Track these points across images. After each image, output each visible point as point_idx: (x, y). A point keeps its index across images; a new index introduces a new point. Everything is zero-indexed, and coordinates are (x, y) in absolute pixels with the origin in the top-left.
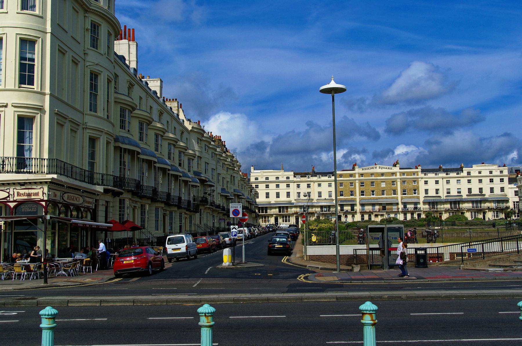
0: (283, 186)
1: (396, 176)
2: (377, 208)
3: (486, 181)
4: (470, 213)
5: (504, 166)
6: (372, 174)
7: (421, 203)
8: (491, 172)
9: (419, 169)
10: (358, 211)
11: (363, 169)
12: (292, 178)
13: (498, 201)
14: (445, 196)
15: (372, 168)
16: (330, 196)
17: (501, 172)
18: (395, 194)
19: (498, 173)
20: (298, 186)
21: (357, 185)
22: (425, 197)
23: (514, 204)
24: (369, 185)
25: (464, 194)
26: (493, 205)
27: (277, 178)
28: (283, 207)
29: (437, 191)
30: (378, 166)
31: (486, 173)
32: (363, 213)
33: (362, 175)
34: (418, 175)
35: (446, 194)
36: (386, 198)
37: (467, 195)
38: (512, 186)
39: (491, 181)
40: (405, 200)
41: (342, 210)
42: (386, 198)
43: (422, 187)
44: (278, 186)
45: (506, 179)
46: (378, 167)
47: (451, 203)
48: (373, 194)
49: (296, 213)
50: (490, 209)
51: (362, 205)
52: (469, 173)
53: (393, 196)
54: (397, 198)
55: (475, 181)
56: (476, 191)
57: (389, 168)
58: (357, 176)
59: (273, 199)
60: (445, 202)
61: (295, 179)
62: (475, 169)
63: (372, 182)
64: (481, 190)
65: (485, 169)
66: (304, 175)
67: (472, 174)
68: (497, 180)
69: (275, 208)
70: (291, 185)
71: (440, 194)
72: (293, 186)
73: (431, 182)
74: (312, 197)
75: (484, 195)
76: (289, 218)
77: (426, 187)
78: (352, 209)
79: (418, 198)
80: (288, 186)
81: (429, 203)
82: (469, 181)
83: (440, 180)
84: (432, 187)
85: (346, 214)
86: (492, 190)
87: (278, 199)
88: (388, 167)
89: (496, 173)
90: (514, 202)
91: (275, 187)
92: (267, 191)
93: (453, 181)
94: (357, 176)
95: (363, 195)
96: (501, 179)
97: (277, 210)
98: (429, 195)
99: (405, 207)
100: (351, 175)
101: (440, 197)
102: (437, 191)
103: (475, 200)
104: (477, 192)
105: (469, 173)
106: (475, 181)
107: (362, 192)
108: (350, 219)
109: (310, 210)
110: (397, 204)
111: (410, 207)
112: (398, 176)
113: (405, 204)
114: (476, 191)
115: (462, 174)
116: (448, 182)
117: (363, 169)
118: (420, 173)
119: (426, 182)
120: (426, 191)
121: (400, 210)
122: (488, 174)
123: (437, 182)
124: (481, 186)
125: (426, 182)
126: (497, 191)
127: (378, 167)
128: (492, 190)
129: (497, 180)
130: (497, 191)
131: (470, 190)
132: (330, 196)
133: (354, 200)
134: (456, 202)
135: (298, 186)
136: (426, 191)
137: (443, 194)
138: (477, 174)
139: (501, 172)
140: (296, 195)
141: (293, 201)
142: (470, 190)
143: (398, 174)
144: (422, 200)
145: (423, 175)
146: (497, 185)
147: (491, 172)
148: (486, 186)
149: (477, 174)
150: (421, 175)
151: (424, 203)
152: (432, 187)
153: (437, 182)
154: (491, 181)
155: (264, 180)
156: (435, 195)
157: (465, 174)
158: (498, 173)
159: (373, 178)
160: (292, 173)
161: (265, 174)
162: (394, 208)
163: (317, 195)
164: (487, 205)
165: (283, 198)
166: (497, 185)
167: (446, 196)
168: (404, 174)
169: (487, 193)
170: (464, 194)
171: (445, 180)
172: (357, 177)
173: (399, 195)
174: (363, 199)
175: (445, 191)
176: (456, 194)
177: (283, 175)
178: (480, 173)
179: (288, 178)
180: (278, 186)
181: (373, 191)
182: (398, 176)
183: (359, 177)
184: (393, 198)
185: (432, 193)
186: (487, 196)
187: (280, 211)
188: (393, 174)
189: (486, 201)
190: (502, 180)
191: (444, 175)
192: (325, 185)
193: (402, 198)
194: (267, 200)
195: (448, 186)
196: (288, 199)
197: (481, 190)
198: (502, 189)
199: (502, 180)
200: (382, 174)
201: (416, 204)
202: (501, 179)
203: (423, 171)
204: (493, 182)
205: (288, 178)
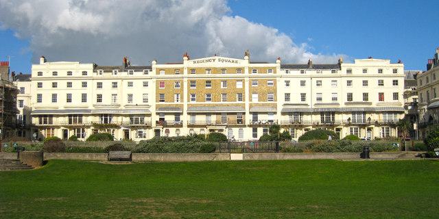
0: (77, 84)
1: (243, 73)
2: (213, 118)
3: (373, 83)
5: (399, 63)
8: (380, 71)
9: (278, 65)
12: (90, 73)
13: (390, 113)
14: (313, 104)
15: (209, 61)
16: (145, 100)
17: (395, 71)
18: (240, 99)
21: (185, 85)
22: (285, 105)
24: (204, 87)
25: (342, 103)
27: (70, 73)
29: (303, 96)
30: (217, 58)
31: (373, 71)
32: (191, 126)
33: (193, 71)
34: (275, 72)
35: (315, 101)
36: (231, 104)
37: (346, 104)
43: (281, 90)
45: (401, 82)
46: (217, 60)
47: (322, 113)
48: (209, 100)
49: (95, 125)
50: (377, 124)
52: (349, 71)
53: (238, 102)
55: (357, 83)
56: (358, 97)
57: (233, 62)
58: (186, 71)
62: (359, 65)
63: (208, 82)
64: (366, 96)
65: (373, 65)
67: (354, 73)
69: (64, 116)
70: (89, 83)
71: (308, 101)
72: (92, 85)
73: (295, 83)
74: (118, 102)
75: (370, 104)
77: (288, 90)
78: (177, 119)
79: (275, 106)
82: (349, 83)
83: (308, 81)
84: (295, 91)
86: (381, 97)
87: (69, 104)
88: (231, 59)
89: (388, 71)
92: (54, 92)
93: (326, 83)
94: (186, 71)
95: (193, 100)
97: (67, 119)
98: (292, 101)
99: (255, 119)
101: (307, 105)
102: (303, 96)
103: (357, 110)
104: (361, 99)
105: (349, 71)
106: (357, 83)
113: (255, 114)
114: (358, 97)
115: (339, 73)
117: (195, 62)
118: (278, 70)
119: (288, 84)
120: (287, 96)
121: (247, 123)
122: (376, 73)
123: (303, 83)
124: (365, 89)
125: (288, 84)
128: (381, 97)
131: (350, 97)
132: (145, 100)
133: (180, 107)
134: (328, 114)
136: (287, 96)
137: (311, 103)
139: (395, 71)
141: (91, 108)
142: (350, 97)
143: (247, 70)
144: (280, 109)
145: (283, 72)
147: (380, 71)
148: (373, 91)
151: (283, 114)
152: (295, 91)
153: (303, 83)
156: (300, 101)
157: (343, 71)
159: (210, 75)
160: (91, 66)
163: (126, 98)
164: (375, 117)
165: (77, 103)
167: (316, 104)
168: (255, 71)
169: (374, 100)
170: (342, 103)
171: (314, 80)
174: (193, 106)
175: (315, 96)
176: (331, 102)
177: (77, 68)
178: (365, 71)
179: (85, 73)
181: (209, 95)
183: (188, 73)
184: (237, 105)
185: (295, 99)
186: (374, 106)
188: (240, 70)
190: (395, 83)
191: (313, 73)
192: (138, 84)
193: (251, 106)
194: (54, 105)
195: (319, 89)
196: (84, 104)
197: (366, 96)
199: (395, 83)
200: (223, 70)
203: (283, 67)
204: (397, 84)
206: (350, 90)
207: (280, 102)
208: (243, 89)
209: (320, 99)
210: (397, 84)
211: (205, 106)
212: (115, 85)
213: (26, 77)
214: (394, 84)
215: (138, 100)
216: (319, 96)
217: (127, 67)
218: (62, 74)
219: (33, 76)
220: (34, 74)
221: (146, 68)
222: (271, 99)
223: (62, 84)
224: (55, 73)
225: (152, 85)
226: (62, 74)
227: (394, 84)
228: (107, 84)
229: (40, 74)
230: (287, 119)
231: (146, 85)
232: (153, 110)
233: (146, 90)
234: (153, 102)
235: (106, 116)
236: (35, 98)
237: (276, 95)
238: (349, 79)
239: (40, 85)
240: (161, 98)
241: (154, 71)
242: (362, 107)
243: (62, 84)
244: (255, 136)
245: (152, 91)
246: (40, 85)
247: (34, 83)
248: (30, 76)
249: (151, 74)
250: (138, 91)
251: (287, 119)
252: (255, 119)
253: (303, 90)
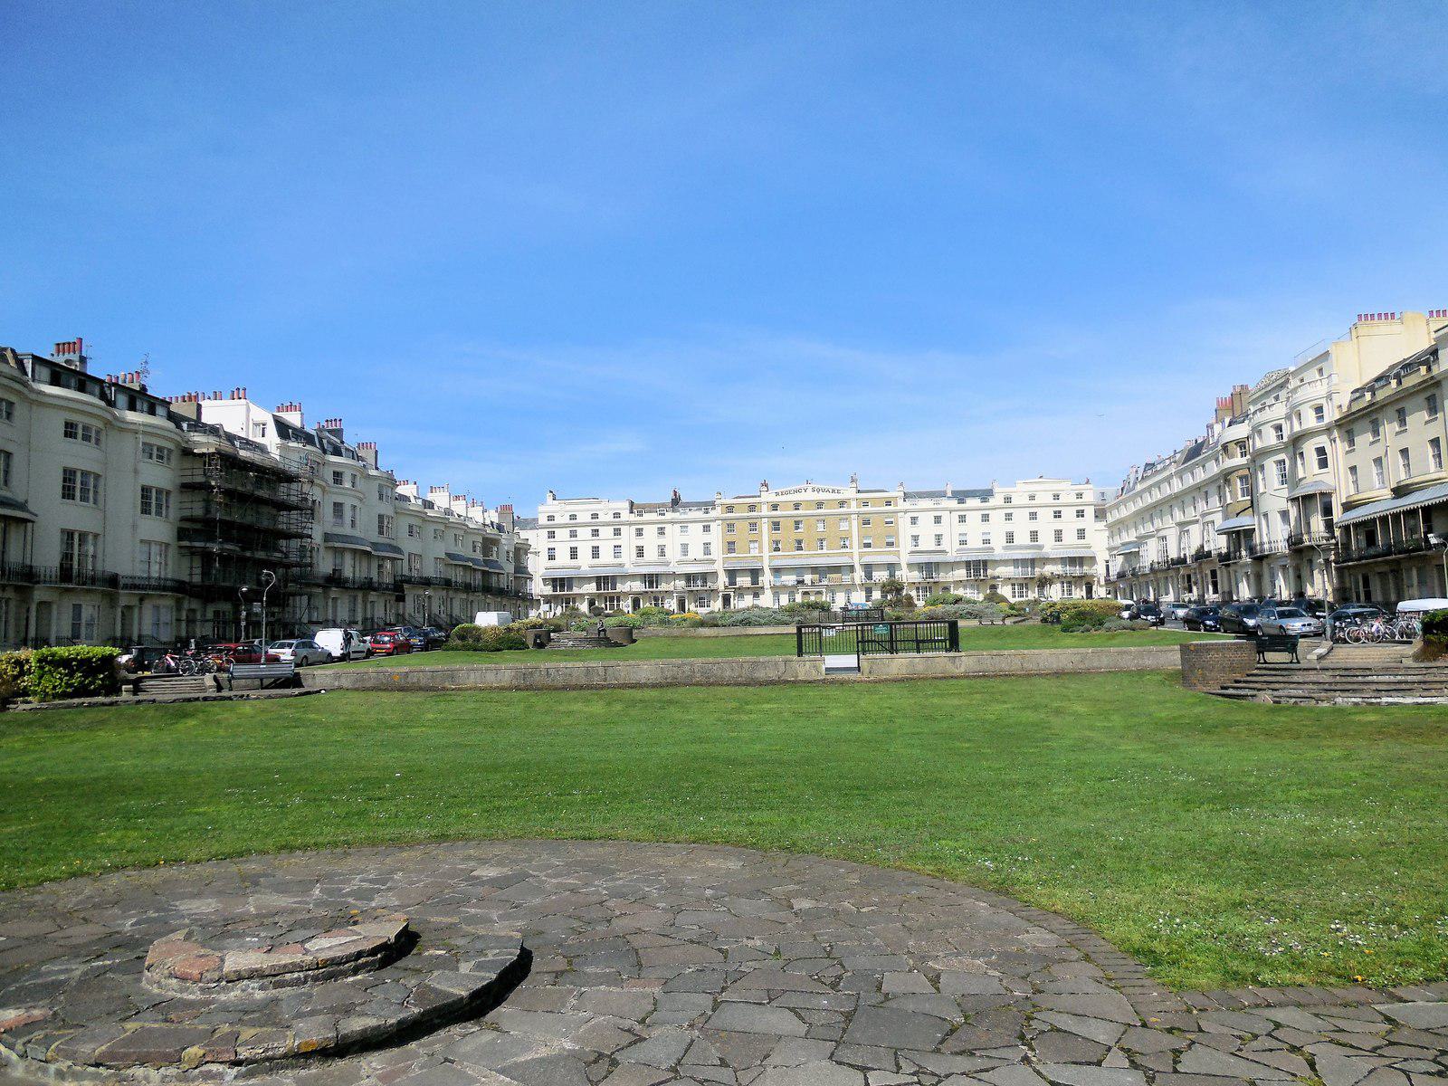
3: (1045, 515)
4: (1010, 587)
5: (1087, 483)
7: (904, 566)
8: (1056, 497)
10: (767, 586)
11: (777, 494)
12: (626, 515)
13: (1073, 561)
16: (707, 552)
17: (1080, 496)
19: (1073, 499)
20: (639, 533)
23: (1108, 567)
26: (1057, 569)
28: (606, 578)
29: (939, 538)
32: (777, 591)
33: (775, 507)
35: (956, 545)
37: (1005, 548)
38: (1101, 525)
39: (1058, 515)
40: (867, 560)
41: (732, 582)
42: (828, 555)
43: (905, 530)
44: (595, 533)
45: (1089, 512)
46: (810, 490)
51: (777, 571)
52: (1008, 500)
54: (851, 555)
55: (1021, 516)
56: (1022, 538)
57: (833, 491)
58: (765, 507)
59: (585, 563)
60: (1005, 562)
61: (633, 518)
66: (651, 508)
67: (1014, 502)
68: (1069, 513)
69: (588, 580)
70: (624, 529)
71: (945, 545)
73: (926, 520)
75: (1040, 547)
76: (618, 601)
78: (755, 581)
79: (897, 554)
80: (617, 532)
81: (920, 567)
82: (1009, 517)
83: (945, 516)
84: (926, 529)
85: (741, 592)
86: (1058, 535)
90: (1107, 562)
91: (590, 537)
92: (573, 545)
93: (974, 518)
94: (765, 507)
95: (777, 549)
96: (1078, 512)
99: (869, 576)
100: (752, 508)
101: (944, 551)
102: (939, 538)
103: (1020, 557)
104: (1027, 541)
105: (1008, 500)
106: (1021, 516)
107: (777, 542)
108: (748, 601)
109: (663, 587)
110: (852, 569)
111: (881, 576)
112: (854, 507)
114: (1022, 538)
115: (992, 502)
116: (962, 519)
117: (777, 494)
119: (914, 521)
121: (858, 581)
122: (1050, 500)
123: (938, 520)
125: (914, 521)
126: (1070, 537)
127: (810, 490)
128: (1058, 535)
129: (1069, 513)
130: (1070, 537)
131: (1010, 537)
132: (707, 552)
134: (977, 567)
135: (639, 533)
138: (1026, 501)
139: (1080, 496)
140: (634, 552)
142: (1010, 537)
143: (853, 504)
144: (904, 559)
146: (1069, 524)
147: (1056, 497)
148: (1046, 525)
149: (1026, 501)
150: (902, 505)
154: (1058, 515)
155: (566, 520)
157: (997, 500)
158: (1073, 499)
160: (627, 505)
161: (569, 508)
162: (846, 578)
166: (1069, 524)
168: (866, 504)
169: (1047, 540)
171: (955, 515)
172: (765, 511)
173: (856, 549)
176: (981, 545)
178: (1032, 498)
179: (617, 515)
180: (595, 533)
181: (799, 542)
182: (854, 507)
185: (927, 543)
187: (599, 588)
189: (1046, 561)
190: (1080, 514)
191: (954, 504)
193: (861, 555)
195: (963, 528)
198: (1081, 534)
199: (1080, 514)
200: (820, 505)
201: (892, 567)
202: (1078, 512)
203: (906, 496)
205: (617, 515)
206: (1009, 527)
207: (905, 546)
208: (849, 531)
209: (963, 542)
210: (1083, 516)
211: (794, 557)
212: (661, 532)
213: (532, 524)
214: (1078, 516)
215: (696, 552)
216: (963, 538)
218: (584, 517)
219: (540, 522)
220: (543, 520)
221: (706, 504)
222: (890, 544)
223: (584, 533)
224: (573, 517)
225: (716, 528)
226: (584, 517)
227: (1055, 517)
228: (650, 531)
229: (551, 518)
230: (916, 576)
231: (707, 529)
232: (719, 567)
233: (707, 538)
234: (717, 551)
235: (651, 579)
236: (545, 555)
237: (897, 538)
238: (1009, 511)
239: (552, 535)
240: (731, 546)
241: (719, 509)
242: (1028, 554)
243: (584, 533)
244: (868, 598)
245: (717, 536)
246: (552, 535)
247: (544, 533)
248: (536, 520)
249: (713, 514)
251: (916, 576)
252: (869, 576)
253: (938, 529)
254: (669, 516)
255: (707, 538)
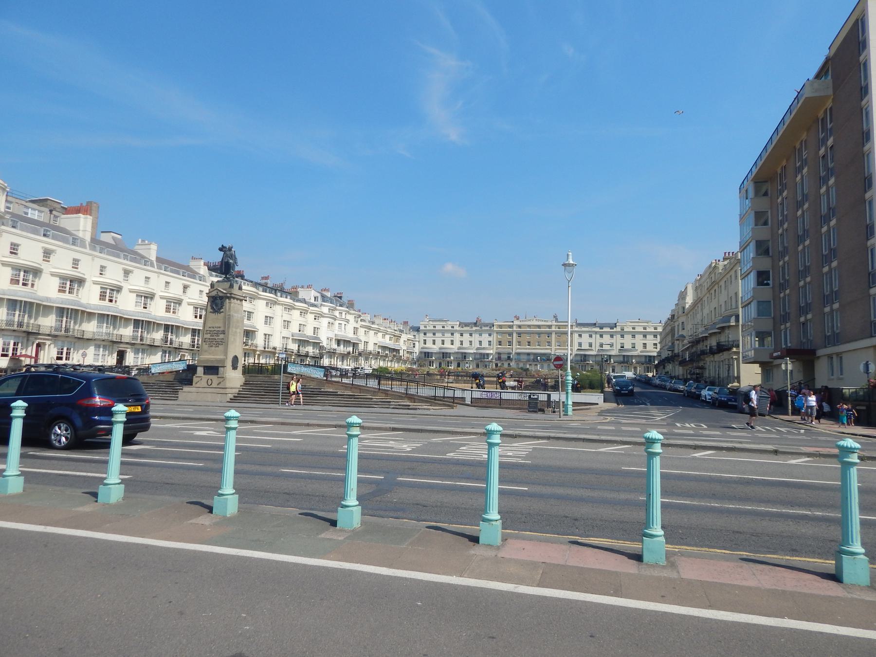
6: (529, 326)
12: (457, 328)
33: (520, 327)
66: (467, 325)
71: (593, 348)
72: (457, 335)
114: (628, 346)
115: (615, 330)
120: (580, 344)
125: (580, 336)
136: (580, 344)
157: (618, 329)
175: (598, 345)
182: (553, 329)
191: (597, 329)
200: (539, 327)
217: (475, 324)
220: (422, 328)
245: (494, 338)
250: (485, 338)
253: (591, 340)
254: (474, 328)
255: (491, 339)
